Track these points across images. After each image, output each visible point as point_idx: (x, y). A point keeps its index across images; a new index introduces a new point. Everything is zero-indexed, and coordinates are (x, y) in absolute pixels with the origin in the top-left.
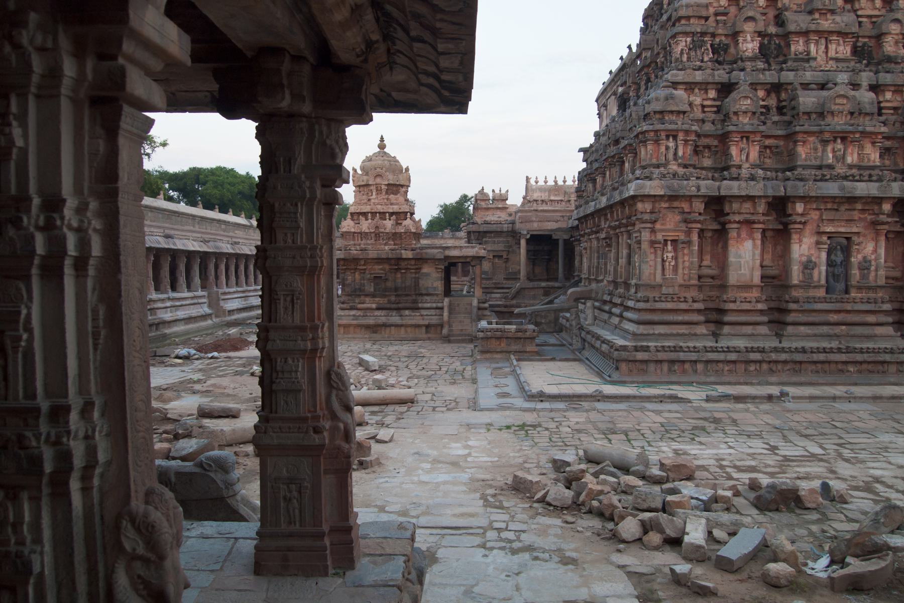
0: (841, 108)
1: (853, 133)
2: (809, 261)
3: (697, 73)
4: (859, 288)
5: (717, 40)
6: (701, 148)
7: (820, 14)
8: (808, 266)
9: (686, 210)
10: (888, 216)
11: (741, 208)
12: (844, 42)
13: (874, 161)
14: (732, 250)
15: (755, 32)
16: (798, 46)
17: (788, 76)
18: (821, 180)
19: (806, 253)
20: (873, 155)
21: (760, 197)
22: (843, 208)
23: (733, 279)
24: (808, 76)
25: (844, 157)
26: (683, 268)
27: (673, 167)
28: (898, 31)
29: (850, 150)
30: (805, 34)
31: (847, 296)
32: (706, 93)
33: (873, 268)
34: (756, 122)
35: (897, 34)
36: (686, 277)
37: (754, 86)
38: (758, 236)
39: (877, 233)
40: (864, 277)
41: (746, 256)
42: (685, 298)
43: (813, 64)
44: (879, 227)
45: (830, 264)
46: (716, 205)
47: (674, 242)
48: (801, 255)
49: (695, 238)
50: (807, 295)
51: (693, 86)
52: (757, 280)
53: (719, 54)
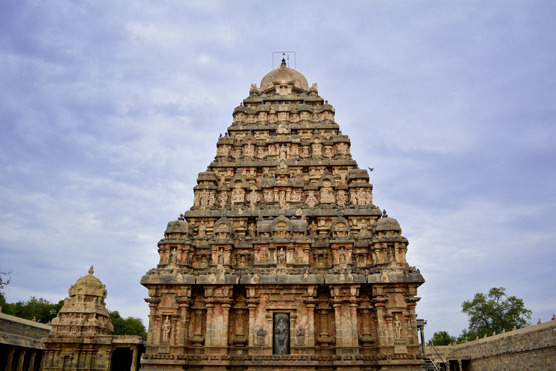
0: (281, 229)
1: (289, 243)
2: (262, 330)
4: (296, 349)
8: (262, 334)
9: (179, 295)
11: (213, 293)
14: (208, 322)
15: (242, 188)
19: (260, 325)
20: (305, 258)
22: (282, 292)
23: (208, 344)
24: (270, 212)
25: (286, 260)
26: (175, 336)
28: (329, 186)
31: (287, 355)
33: (306, 335)
34: (228, 238)
38: (226, 312)
40: (301, 342)
42: (173, 356)
44: (308, 306)
47: (170, 316)
49: (184, 313)
50: (258, 354)
51: (200, 220)
52: (224, 344)
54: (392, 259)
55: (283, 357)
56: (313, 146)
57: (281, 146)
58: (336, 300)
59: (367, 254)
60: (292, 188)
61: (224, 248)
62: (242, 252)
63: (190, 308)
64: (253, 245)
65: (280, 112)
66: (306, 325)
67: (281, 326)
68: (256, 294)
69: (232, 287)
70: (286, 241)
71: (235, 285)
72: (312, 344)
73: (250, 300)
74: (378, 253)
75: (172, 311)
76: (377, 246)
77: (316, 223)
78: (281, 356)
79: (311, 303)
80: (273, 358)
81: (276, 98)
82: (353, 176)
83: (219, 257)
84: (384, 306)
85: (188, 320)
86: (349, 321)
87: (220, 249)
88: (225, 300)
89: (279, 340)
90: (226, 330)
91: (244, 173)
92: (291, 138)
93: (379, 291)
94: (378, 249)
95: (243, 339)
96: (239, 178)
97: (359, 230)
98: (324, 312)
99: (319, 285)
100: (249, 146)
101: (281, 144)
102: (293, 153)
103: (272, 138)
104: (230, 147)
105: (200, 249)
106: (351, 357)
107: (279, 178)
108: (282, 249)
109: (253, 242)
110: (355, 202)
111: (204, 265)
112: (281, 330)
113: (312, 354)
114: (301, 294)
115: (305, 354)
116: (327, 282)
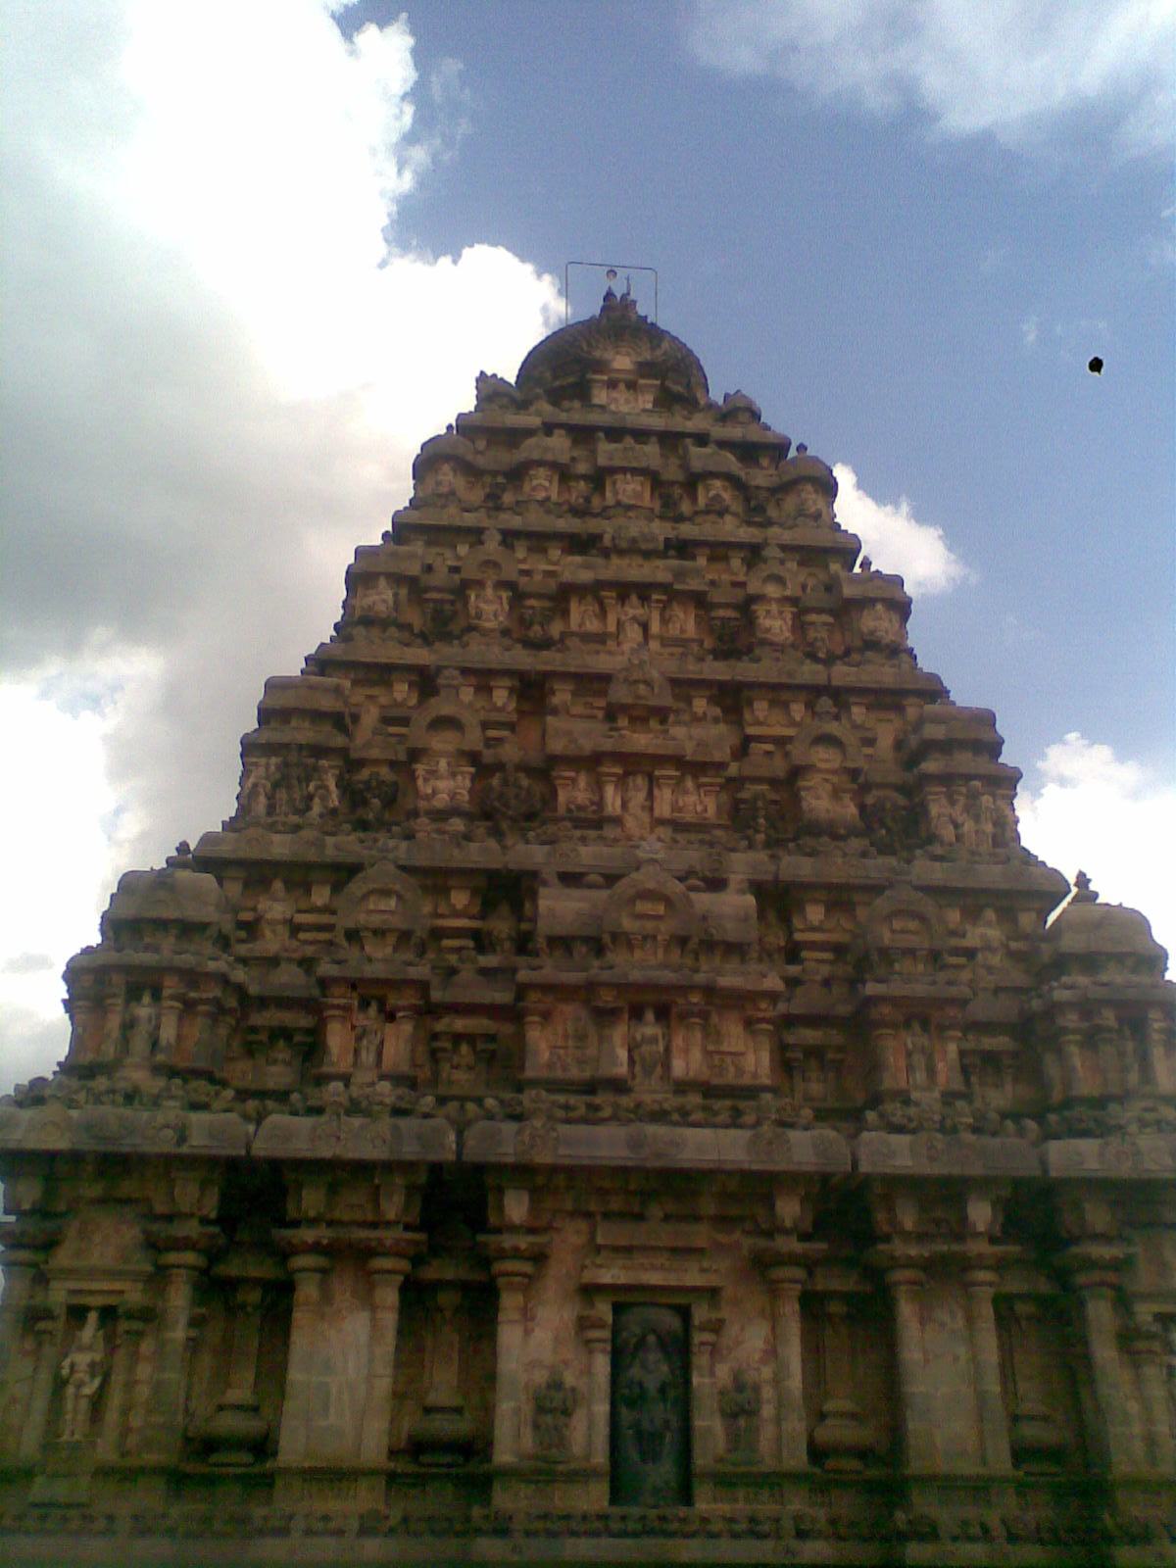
0: (649, 926)
2: (556, 1385)
3: (276, 838)
4: (725, 1481)
5: (365, 774)
6: (263, 1037)
7: (633, 720)
9: (160, 1208)
10: (805, 1237)
12: (699, 786)
13: (755, 1075)
14: (299, 1341)
15: (462, 753)
16: (574, 792)
17: (528, 853)
18: (586, 1121)
20: (756, 1061)
21: (389, 1167)
22: (655, 1211)
23: (292, 1449)
24: (588, 854)
25: (667, 1066)
27: (136, 1074)
28: (836, 765)
29: (678, 1041)
30: (592, 762)
31: (682, 1511)
32: (308, 892)
33: (768, 1411)
35: (834, 772)
36: (132, 1440)
37: (436, 880)
38: (389, 1296)
39: (774, 1290)
41: (345, 1367)
43: (610, 832)
45: (622, 1394)
46: (255, 1194)
47: (108, 1314)
48: (533, 1365)
49: (179, 1299)
53: (365, 803)
54: (1133, 1078)
55: (662, 1519)
56: (760, 609)
57: (623, 598)
58: (900, 1248)
59: (1015, 1055)
60: (678, 761)
61: (382, 1002)
62: (460, 1024)
63: (205, 1272)
64: (522, 990)
65: (612, 471)
66: (763, 1361)
67: (652, 1371)
68: (535, 1208)
69: (422, 1178)
70: (668, 976)
71: (436, 1168)
72: (797, 1459)
73: (508, 1241)
74: (1074, 1049)
75: (117, 1286)
76: (1071, 1019)
77: (785, 919)
78: (653, 1513)
79: (793, 1260)
80: (615, 1526)
81: (594, 418)
82: (933, 732)
83: (359, 1039)
84: (1117, 1289)
85: (193, 1333)
86: (962, 1351)
87: (365, 1004)
88: (389, 1236)
89: (639, 1434)
90: (384, 1384)
91: (467, 694)
92: (659, 571)
93: (1098, 1216)
94: (1074, 1031)
95: (458, 1427)
96: (446, 709)
97: (970, 953)
98: (836, 1308)
99: (825, 1178)
100: (489, 592)
101: (625, 590)
102: (674, 630)
103: (587, 567)
104: (404, 592)
105: (263, 1002)
106: (985, 1530)
107: (623, 722)
108: (650, 1016)
109: (523, 976)
110: (948, 833)
111: (278, 1073)
112: (652, 1385)
113: (797, 1503)
114: (741, 1219)
115: (766, 1507)
116: (865, 1167)
